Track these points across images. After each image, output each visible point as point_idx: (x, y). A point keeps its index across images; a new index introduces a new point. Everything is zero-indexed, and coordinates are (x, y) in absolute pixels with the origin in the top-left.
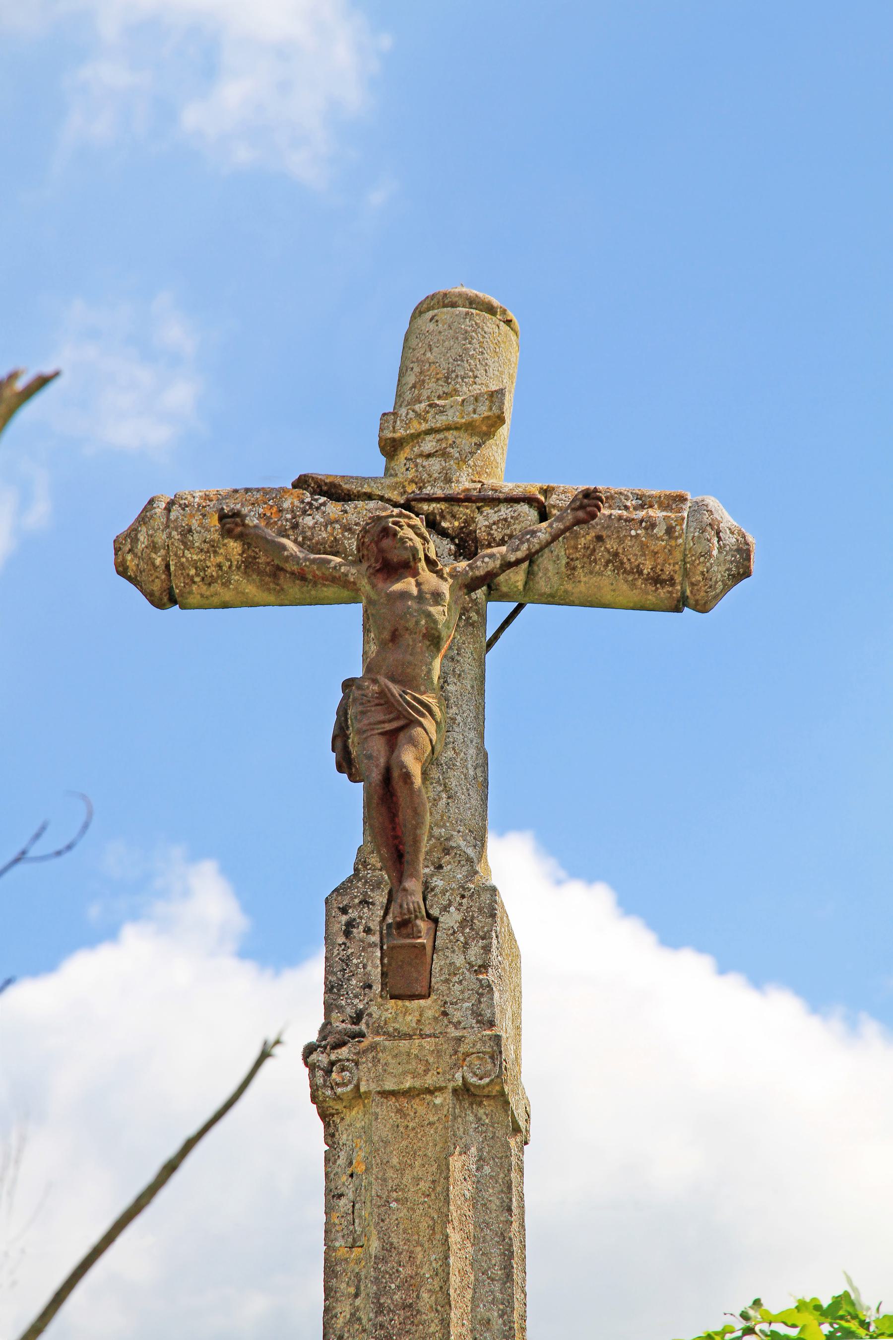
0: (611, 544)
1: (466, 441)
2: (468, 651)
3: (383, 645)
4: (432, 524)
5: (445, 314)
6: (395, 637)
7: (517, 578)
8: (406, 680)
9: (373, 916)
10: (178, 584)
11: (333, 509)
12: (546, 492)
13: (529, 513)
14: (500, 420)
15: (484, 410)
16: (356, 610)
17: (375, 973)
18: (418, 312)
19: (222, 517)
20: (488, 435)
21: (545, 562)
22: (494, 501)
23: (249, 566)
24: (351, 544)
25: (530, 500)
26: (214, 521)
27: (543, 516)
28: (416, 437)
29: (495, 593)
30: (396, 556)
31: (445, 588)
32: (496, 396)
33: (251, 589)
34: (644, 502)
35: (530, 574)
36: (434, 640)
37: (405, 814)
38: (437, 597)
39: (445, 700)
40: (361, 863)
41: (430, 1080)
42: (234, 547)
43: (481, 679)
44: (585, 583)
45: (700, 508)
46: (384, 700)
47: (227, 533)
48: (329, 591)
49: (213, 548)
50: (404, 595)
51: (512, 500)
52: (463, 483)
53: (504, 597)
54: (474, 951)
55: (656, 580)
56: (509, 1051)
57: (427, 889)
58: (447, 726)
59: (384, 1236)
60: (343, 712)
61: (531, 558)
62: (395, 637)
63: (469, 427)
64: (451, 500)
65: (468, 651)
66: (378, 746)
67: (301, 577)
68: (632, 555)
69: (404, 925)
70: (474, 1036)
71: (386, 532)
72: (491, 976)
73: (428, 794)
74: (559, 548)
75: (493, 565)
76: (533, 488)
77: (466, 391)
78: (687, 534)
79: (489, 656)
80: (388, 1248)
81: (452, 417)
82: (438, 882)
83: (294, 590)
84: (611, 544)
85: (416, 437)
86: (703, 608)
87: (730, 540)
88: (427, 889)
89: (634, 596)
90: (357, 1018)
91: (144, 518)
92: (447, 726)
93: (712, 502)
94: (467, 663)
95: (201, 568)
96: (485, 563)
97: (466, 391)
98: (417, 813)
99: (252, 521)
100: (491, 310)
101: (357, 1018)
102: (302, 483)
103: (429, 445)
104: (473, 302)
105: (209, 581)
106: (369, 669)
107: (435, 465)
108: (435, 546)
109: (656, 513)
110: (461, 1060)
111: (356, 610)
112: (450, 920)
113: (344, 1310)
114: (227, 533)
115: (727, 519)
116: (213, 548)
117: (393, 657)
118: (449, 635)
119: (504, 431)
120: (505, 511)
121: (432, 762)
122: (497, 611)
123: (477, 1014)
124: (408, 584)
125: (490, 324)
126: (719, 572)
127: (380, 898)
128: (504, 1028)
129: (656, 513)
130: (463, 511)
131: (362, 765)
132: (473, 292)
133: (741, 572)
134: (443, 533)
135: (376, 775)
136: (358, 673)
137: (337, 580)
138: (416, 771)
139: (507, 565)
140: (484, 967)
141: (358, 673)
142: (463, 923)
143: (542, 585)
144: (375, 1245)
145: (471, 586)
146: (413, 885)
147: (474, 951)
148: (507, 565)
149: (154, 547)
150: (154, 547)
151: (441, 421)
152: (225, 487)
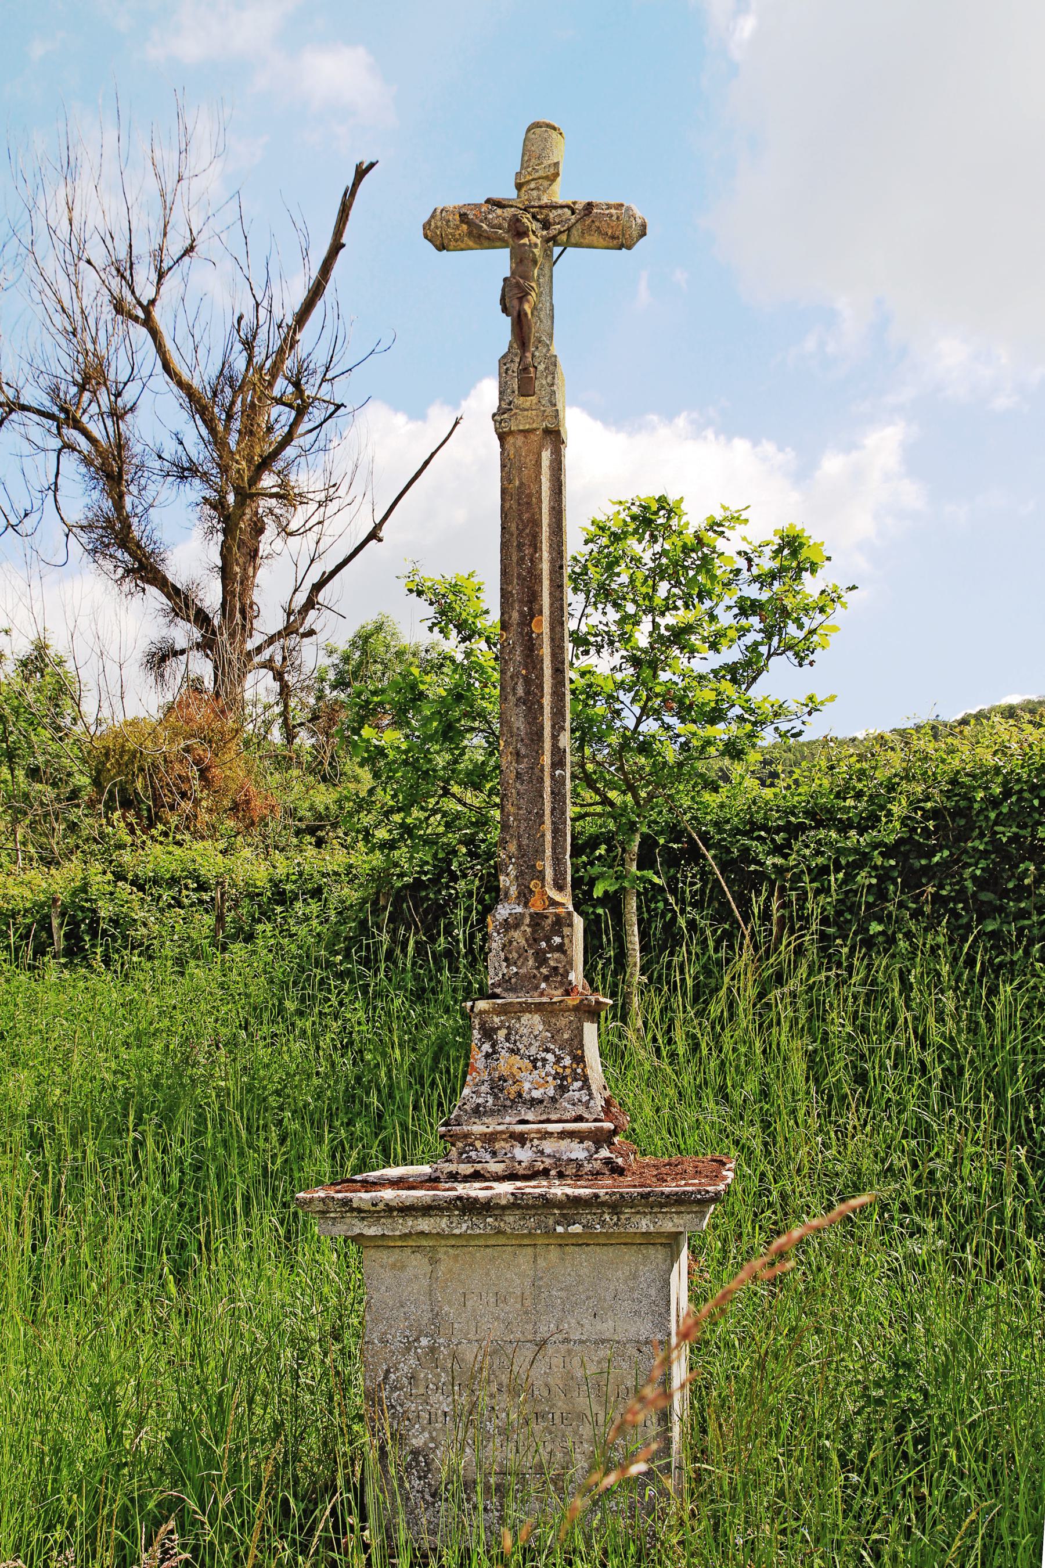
0: (597, 224)
1: (546, 183)
2: (547, 265)
3: (517, 264)
4: (534, 217)
5: (538, 130)
6: (521, 261)
7: (564, 237)
8: (526, 278)
9: (515, 366)
10: (446, 241)
11: (499, 211)
12: (574, 203)
13: (568, 212)
14: (557, 174)
15: (552, 171)
16: (507, 251)
17: (516, 387)
18: (528, 130)
19: (460, 215)
20: (553, 181)
21: (574, 231)
22: (556, 207)
23: (470, 234)
24: (506, 225)
25: (568, 207)
26: (457, 217)
27: (573, 213)
28: (528, 182)
29: (556, 244)
30: (521, 230)
31: (539, 241)
32: (556, 164)
33: (471, 243)
34: (609, 207)
35: (569, 236)
36: (535, 262)
37: (525, 328)
38: (536, 245)
39: (539, 285)
40: (511, 347)
41: (534, 426)
42: (465, 227)
43: (551, 276)
44: (588, 239)
45: (628, 209)
46: (518, 285)
47: (462, 221)
48: (498, 244)
49: (457, 227)
50: (524, 245)
51: (562, 207)
52: (545, 200)
53: (559, 245)
54: (549, 378)
55: (613, 237)
56: (561, 416)
57: (533, 356)
58: (539, 295)
59: (520, 479)
60: (503, 290)
61: (569, 229)
62: (521, 261)
63: (547, 178)
64: (541, 207)
65: (547, 265)
66: (516, 303)
67: (488, 238)
68: (604, 228)
69: (525, 370)
70: (549, 410)
71: (518, 220)
72: (555, 388)
73: (533, 320)
74: (579, 226)
75: (555, 232)
76: (569, 201)
77: (546, 163)
78: (624, 218)
79: (555, 268)
80: (522, 484)
81: (541, 173)
82: (537, 354)
83: (486, 243)
84: (597, 224)
85: (528, 182)
86: (629, 248)
87: (639, 221)
88: (533, 356)
89: (605, 244)
90: (510, 404)
91: (433, 216)
92: (539, 295)
93: (633, 206)
94: (546, 271)
95: (453, 235)
96: (553, 231)
97: (546, 163)
98: (530, 328)
99: (471, 217)
100: (554, 129)
101: (510, 404)
102: (488, 201)
103: (533, 185)
104: (549, 126)
105: (456, 241)
106: (513, 273)
107: (535, 193)
108: (535, 226)
109: (613, 211)
110: (544, 418)
111: (507, 251)
112: (541, 367)
113: (507, 505)
114: (462, 221)
115: (638, 213)
116: (457, 227)
117: (521, 269)
118: (540, 260)
119: (559, 179)
120: (560, 211)
121: (534, 308)
122: (557, 250)
123: (550, 401)
124: (525, 241)
125: (554, 134)
126: (635, 234)
127: (517, 360)
128: (559, 407)
129: (613, 211)
130: (545, 211)
131: (510, 310)
132: (547, 121)
133: (643, 234)
134: (538, 220)
135: (515, 314)
136: (508, 275)
137: (502, 240)
138: (529, 311)
139: (561, 232)
140: (553, 385)
141: (508, 275)
142: (546, 368)
143: (573, 240)
144: (517, 483)
145: (548, 240)
146: (529, 355)
147: (549, 378)
148: (561, 232)
149: (437, 227)
150: (437, 227)
151: (536, 175)
152: (461, 204)
